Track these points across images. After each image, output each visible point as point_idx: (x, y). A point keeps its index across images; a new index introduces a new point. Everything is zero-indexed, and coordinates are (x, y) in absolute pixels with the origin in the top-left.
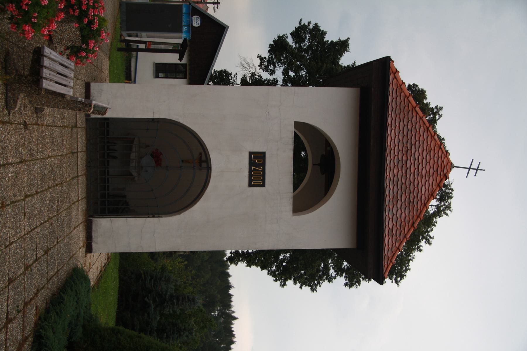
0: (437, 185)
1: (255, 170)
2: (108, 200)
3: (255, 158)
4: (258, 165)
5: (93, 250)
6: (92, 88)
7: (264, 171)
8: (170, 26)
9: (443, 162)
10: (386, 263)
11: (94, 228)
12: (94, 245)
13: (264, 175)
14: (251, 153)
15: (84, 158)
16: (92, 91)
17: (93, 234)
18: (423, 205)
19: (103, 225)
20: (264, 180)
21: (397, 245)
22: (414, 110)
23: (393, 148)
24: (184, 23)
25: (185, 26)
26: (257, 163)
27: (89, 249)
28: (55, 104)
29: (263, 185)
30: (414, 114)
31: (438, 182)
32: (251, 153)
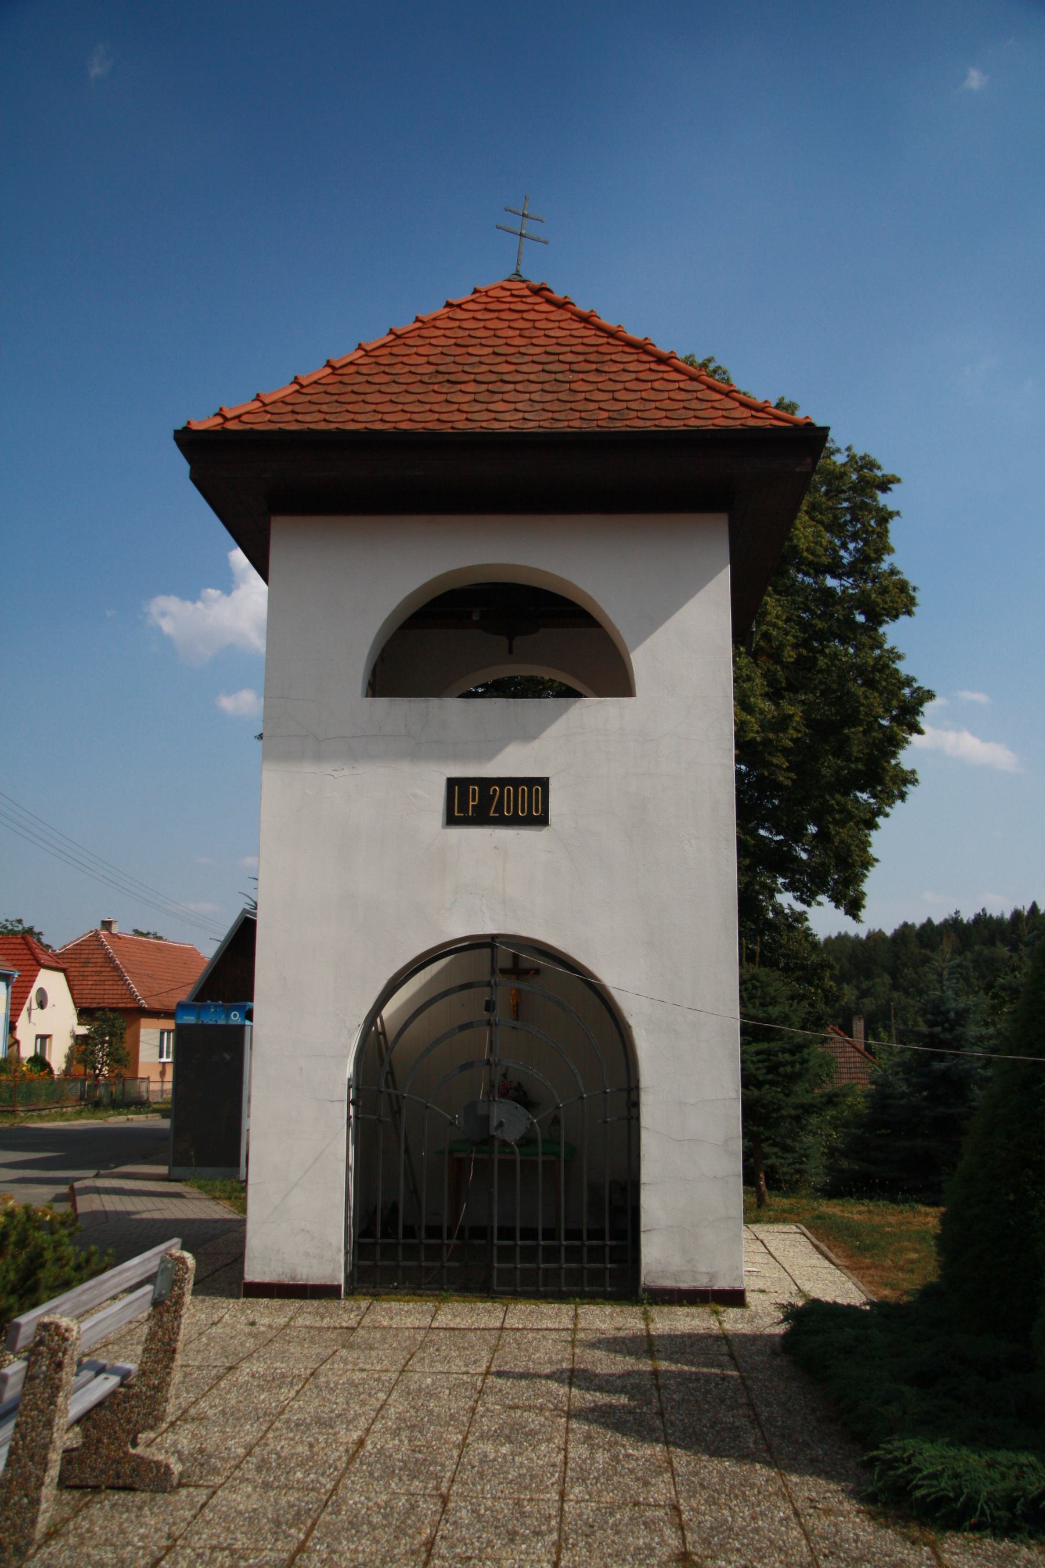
0: (561, 311)
1: (499, 809)
2: (589, 1238)
3: (463, 807)
4: (486, 799)
5: (737, 1286)
6: (258, 1279)
7: (502, 782)
8: (227, 1056)
9: (498, 300)
10: (768, 422)
11: (668, 1283)
12: (723, 1283)
13: (516, 782)
14: (451, 820)
15: (458, 1306)
16: (267, 1279)
17: (684, 1286)
18: (611, 341)
19: (659, 1257)
20: (530, 782)
21: (718, 396)
22: (340, 372)
23: (436, 416)
24: (222, 1022)
25: (228, 1016)
26: (478, 803)
27: (735, 1298)
28: (32, 1457)
29: (544, 783)
30: (352, 369)
31: (552, 308)
32: (451, 820)
